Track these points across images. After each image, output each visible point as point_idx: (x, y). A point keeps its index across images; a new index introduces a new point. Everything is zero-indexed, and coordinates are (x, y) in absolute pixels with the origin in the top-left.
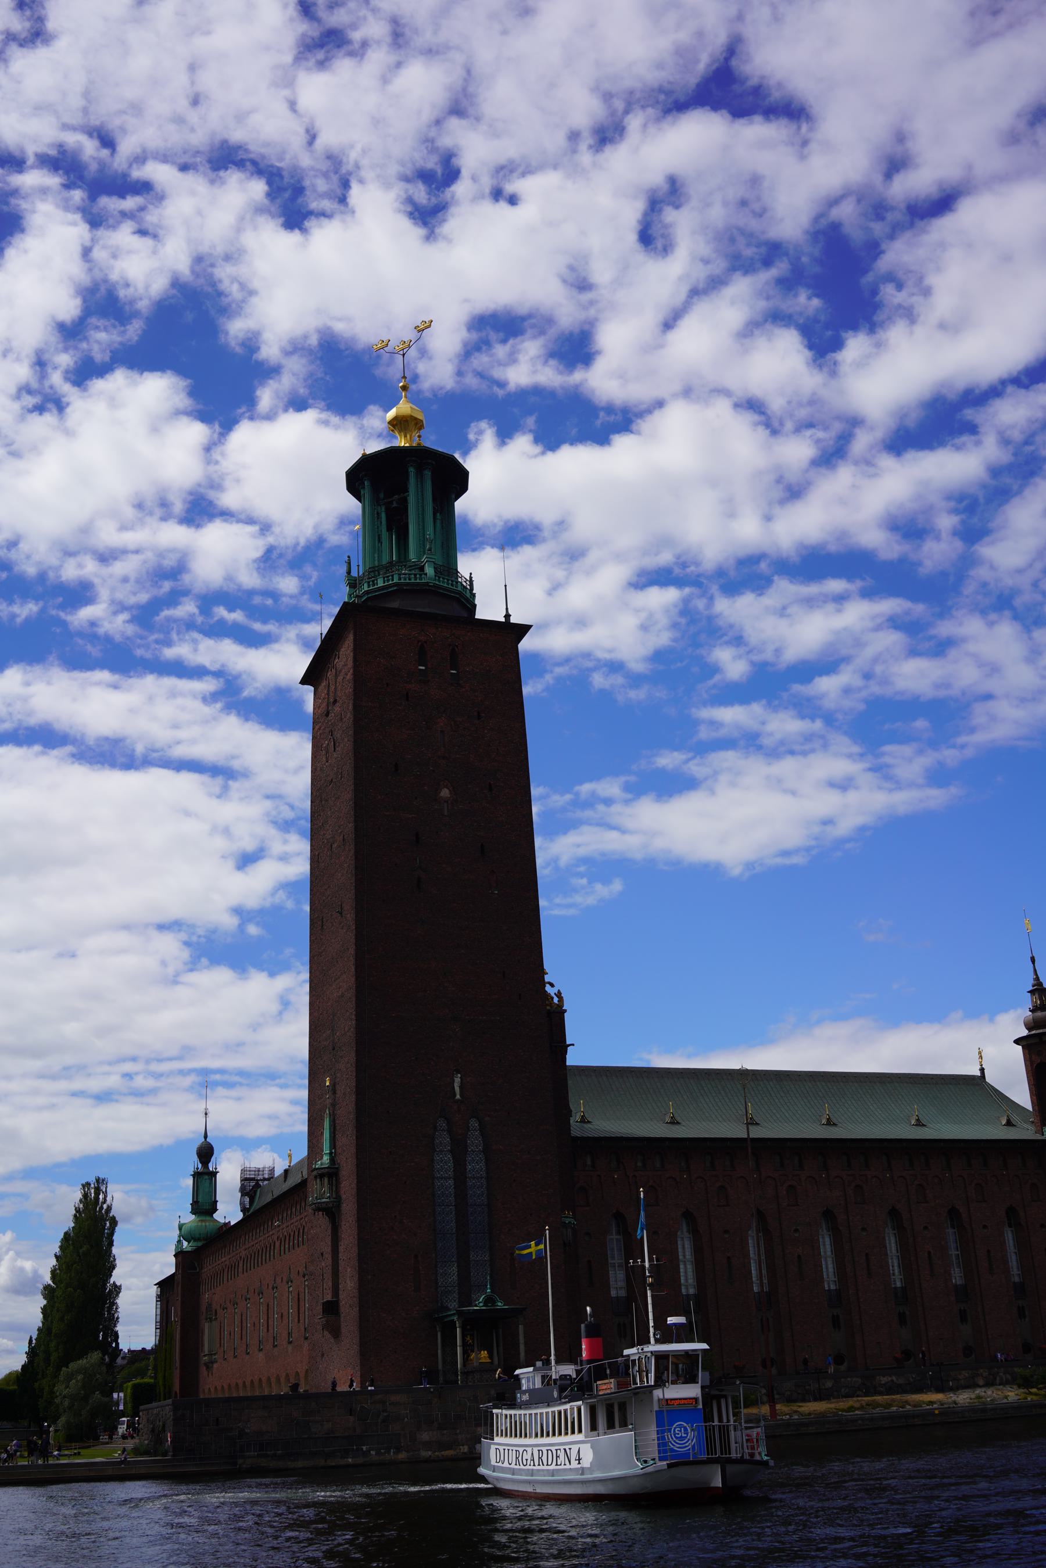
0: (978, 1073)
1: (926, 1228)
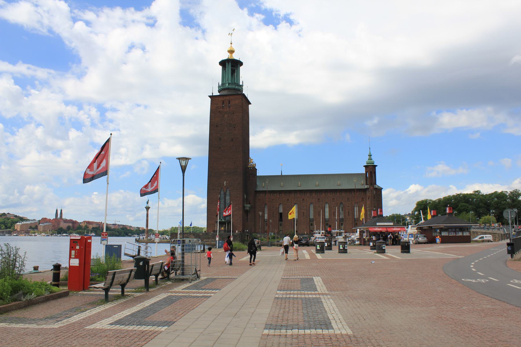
1: (334, 207)
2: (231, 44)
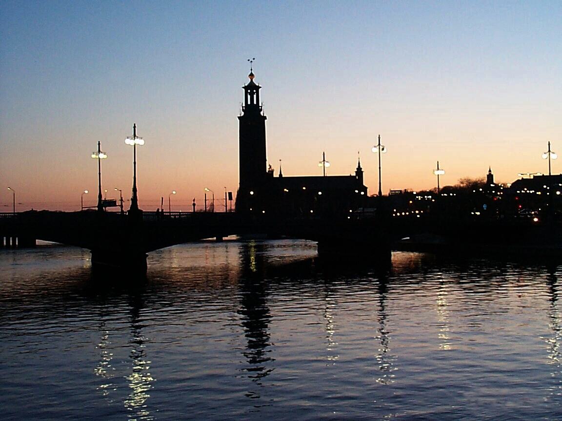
2: (251, 70)
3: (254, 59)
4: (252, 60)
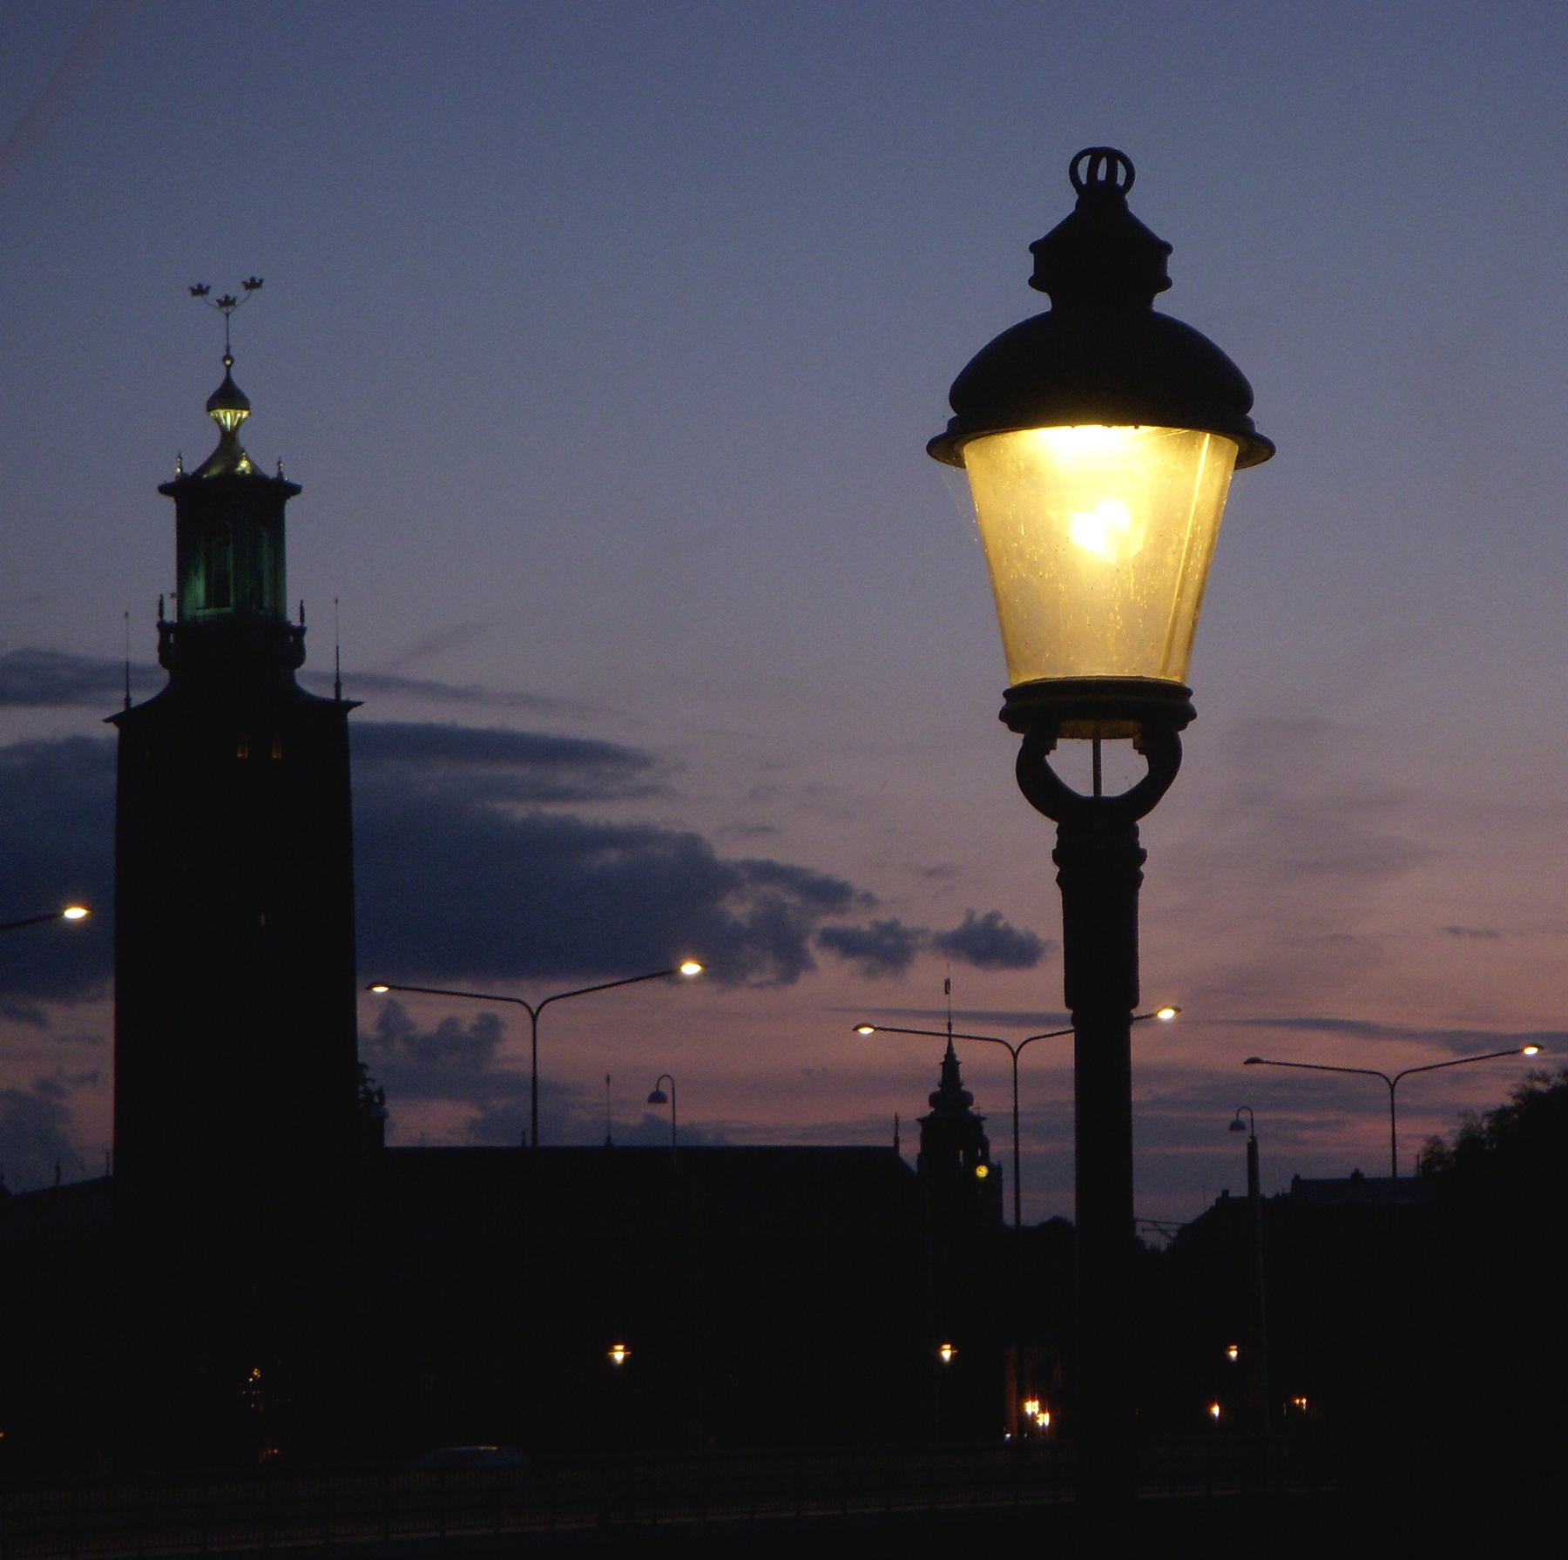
0: (892, 1145)
3: (253, 284)
4: (237, 291)
